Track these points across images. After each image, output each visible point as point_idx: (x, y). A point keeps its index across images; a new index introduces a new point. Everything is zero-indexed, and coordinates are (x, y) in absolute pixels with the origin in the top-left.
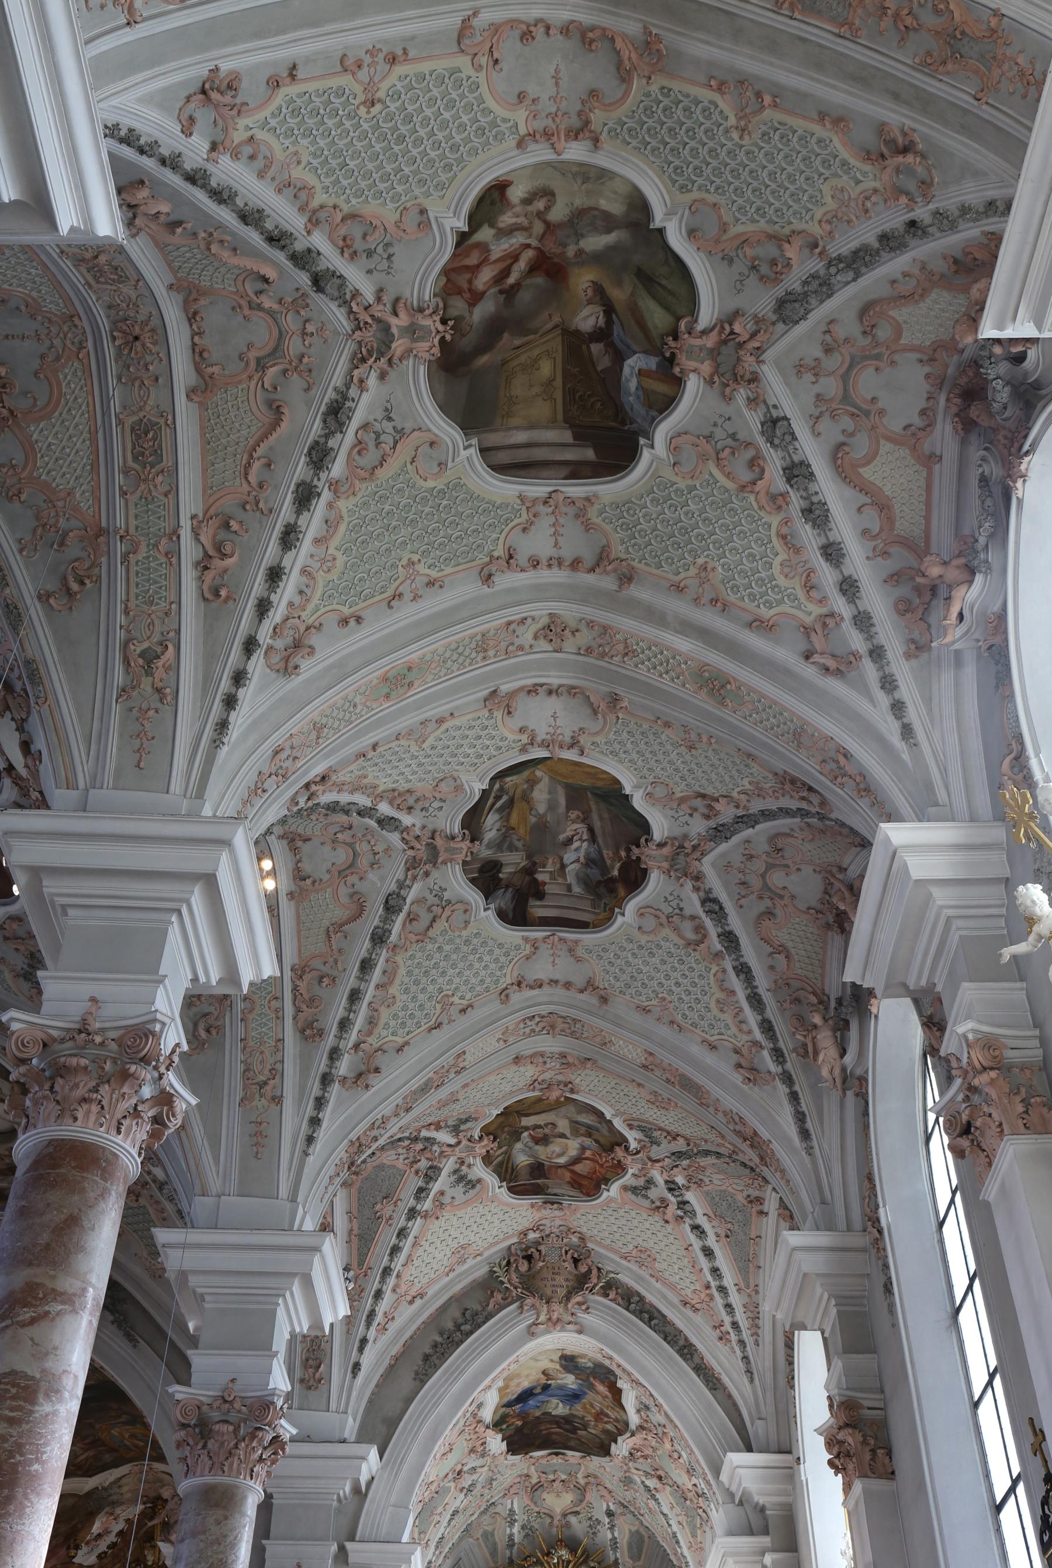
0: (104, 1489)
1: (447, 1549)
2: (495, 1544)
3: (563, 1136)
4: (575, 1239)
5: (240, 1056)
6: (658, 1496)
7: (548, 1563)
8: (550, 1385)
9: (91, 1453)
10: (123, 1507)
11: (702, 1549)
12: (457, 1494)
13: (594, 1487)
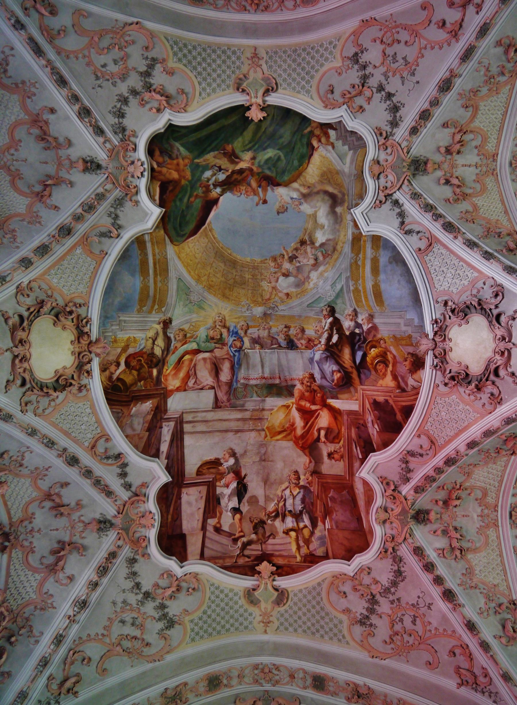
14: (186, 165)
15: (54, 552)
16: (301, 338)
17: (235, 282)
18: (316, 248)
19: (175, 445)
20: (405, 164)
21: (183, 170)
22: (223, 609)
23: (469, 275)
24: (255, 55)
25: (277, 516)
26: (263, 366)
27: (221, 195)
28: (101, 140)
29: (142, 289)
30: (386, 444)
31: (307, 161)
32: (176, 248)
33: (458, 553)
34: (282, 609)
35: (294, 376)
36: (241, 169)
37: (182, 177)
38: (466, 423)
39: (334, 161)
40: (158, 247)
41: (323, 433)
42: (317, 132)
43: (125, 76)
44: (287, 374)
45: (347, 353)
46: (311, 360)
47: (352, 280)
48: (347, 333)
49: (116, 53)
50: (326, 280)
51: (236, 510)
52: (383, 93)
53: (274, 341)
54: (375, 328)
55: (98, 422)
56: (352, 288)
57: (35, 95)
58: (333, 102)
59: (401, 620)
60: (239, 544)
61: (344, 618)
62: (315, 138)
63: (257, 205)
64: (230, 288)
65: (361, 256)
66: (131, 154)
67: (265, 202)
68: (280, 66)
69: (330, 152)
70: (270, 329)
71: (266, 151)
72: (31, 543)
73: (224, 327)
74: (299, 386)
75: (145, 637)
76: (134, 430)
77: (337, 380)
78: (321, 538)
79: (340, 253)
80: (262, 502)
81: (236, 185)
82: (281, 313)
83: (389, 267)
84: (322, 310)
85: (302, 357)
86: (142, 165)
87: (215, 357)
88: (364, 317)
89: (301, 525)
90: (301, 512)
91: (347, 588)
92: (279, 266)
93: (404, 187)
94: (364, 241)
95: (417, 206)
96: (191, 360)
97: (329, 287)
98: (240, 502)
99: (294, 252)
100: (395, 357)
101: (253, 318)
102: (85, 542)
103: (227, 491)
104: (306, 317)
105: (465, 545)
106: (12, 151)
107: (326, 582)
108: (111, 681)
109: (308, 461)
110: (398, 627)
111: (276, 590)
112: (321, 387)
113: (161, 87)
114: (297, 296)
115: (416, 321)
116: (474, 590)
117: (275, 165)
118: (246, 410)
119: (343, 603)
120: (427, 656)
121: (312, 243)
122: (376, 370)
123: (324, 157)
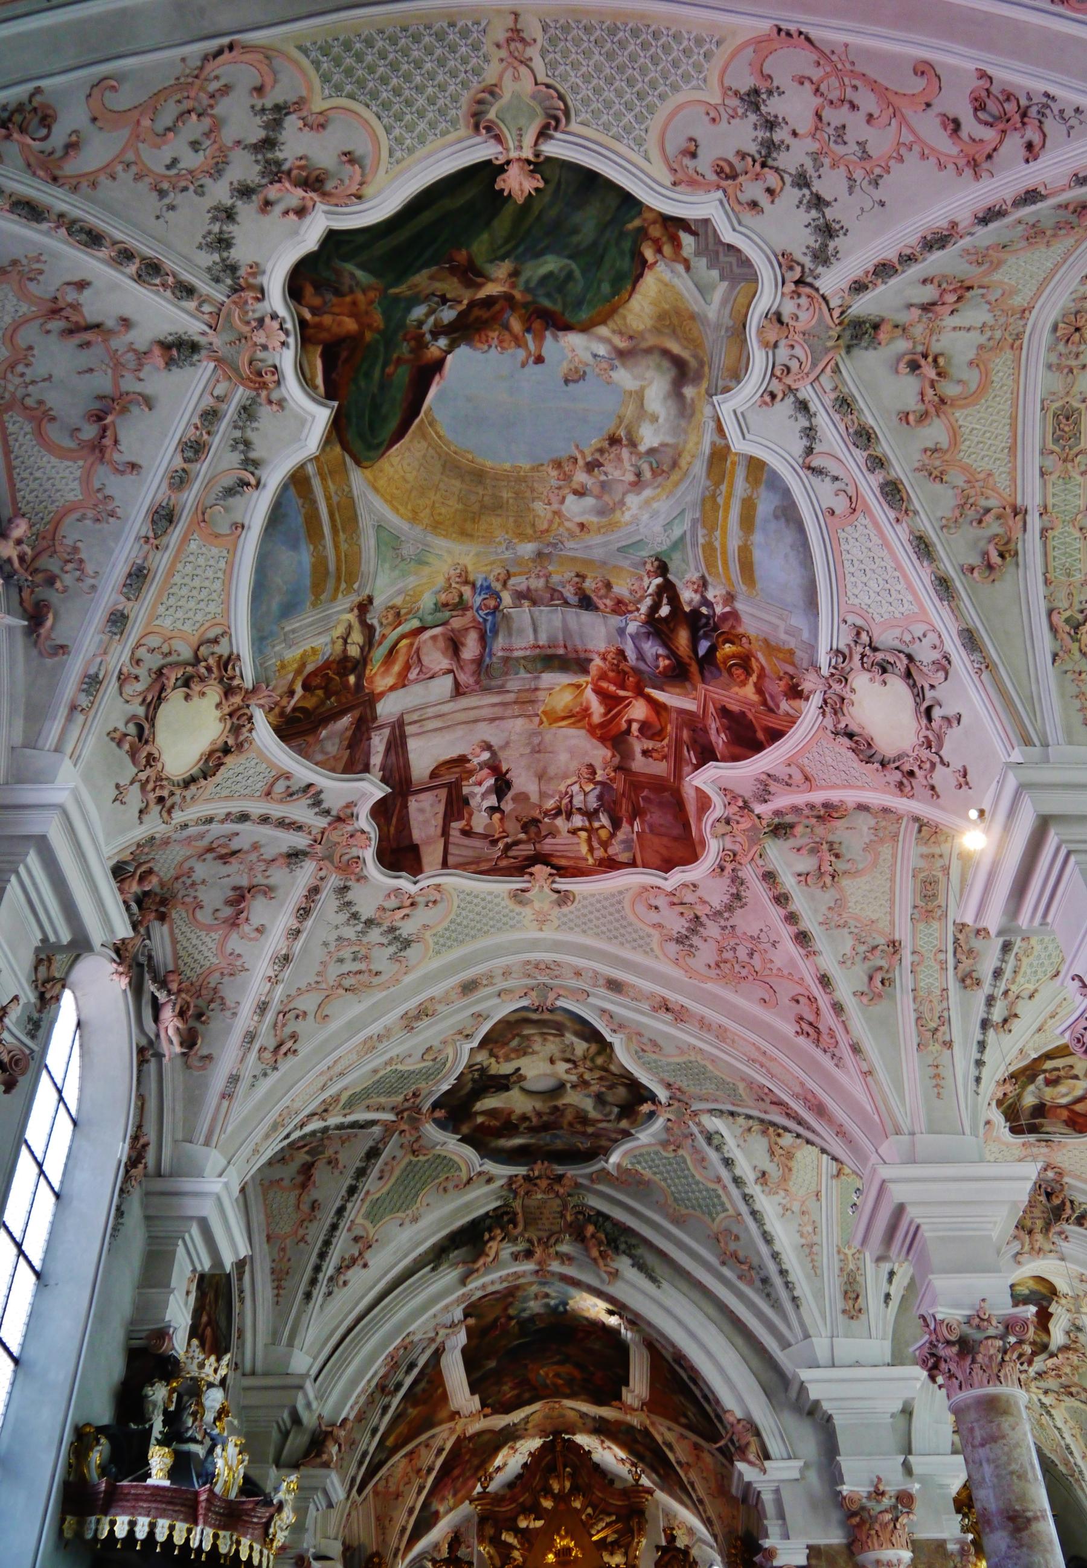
0: (515, 1425)
3: (1076, 1077)
4: (1050, 1174)
5: (912, 1006)
6: (1053, 1412)
9: (515, 1392)
10: (522, 1442)
14: (372, 302)
15: (230, 903)
16: (606, 597)
17: (483, 507)
18: (640, 456)
19: (393, 752)
20: (831, 333)
21: (367, 313)
22: (478, 914)
23: (906, 604)
24: (516, 35)
25: (558, 812)
26: (535, 631)
27: (448, 352)
28: (191, 305)
29: (315, 567)
30: (735, 758)
31: (629, 287)
32: (367, 472)
33: (828, 880)
34: (565, 909)
35: (590, 647)
36: (489, 297)
37: (364, 326)
38: (859, 784)
39: (687, 295)
40: (334, 482)
41: (635, 726)
42: (655, 231)
43: (221, 166)
44: (578, 642)
45: (683, 637)
46: (621, 632)
47: (704, 526)
48: (687, 609)
49: (194, 127)
50: (654, 515)
51: (492, 810)
52: (806, 191)
53: (556, 595)
54: (734, 615)
55: (271, 765)
56: (701, 540)
57: (41, 272)
58: (695, 176)
59: (734, 949)
60: (501, 845)
61: (655, 933)
62: (649, 243)
63: (523, 365)
64: (473, 520)
65: (724, 488)
66: (258, 306)
67: (540, 360)
68: (575, 66)
69: (679, 276)
70: (548, 577)
71: (542, 260)
72: (195, 898)
73: (466, 582)
74: (598, 661)
75: (372, 967)
76: (327, 753)
77: (665, 667)
78: (623, 842)
79: (685, 474)
80: (534, 798)
81: (478, 330)
82: (570, 554)
83: (773, 525)
84: (645, 563)
85: (606, 624)
86: (281, 328)
87: (452, 630)
88: (717, 593)
89: (596, 825)
90: (596, 811)
91: (661, 902)
92: (568, 478)
93: (822, 379)
94: (733, 463)
95: (842, 428)
96: (412, 645)
97: (658, 529)
98: (499, 801)
99: (597, 456)
100: (762, 668)
101: (518, 561)
102: (271, 881)
103: (479, 790)
104: (615, 567)
105: (840, 866)
106: (20, 368)
107: (631, 892)
108: (334, 1026)
109: (609, 754)
110: (728, 955)
111: (558, 892)
112: (636, 671)
113: (303, 162)
114: (599, 529)
115: (806, 635)
116: (839, 930)
117: (561, 288)
118: (508, 692)
119: (654, 917)
120: (762, 992)
121: (633, 444)
122: (731, 674)
123: (666, 285)
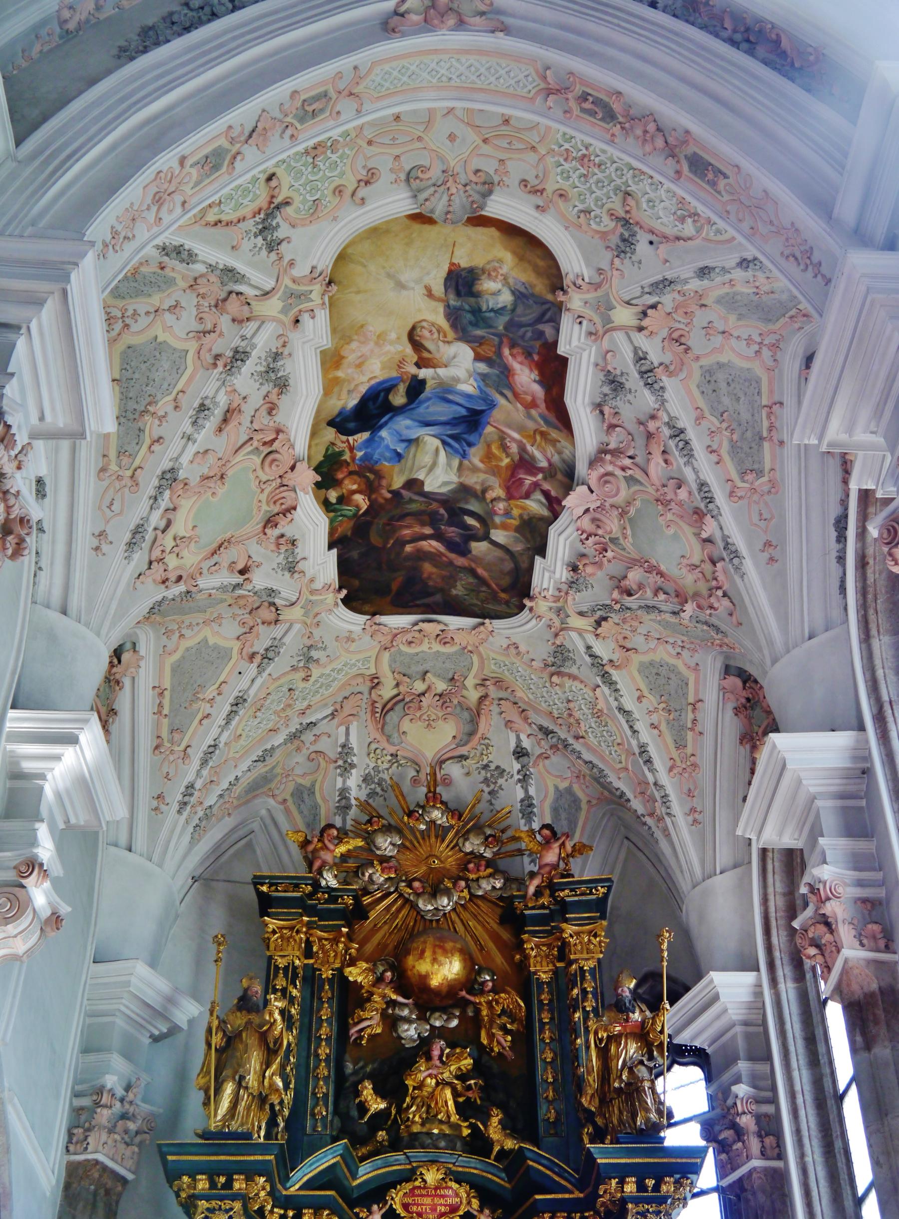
1: (225, 785)
2: (316, 807)
6: (615, 675)
7: (412, 830)
8: (423, 382)
11: (694, 765)
12: (243, 665)
13: (495, 709)
